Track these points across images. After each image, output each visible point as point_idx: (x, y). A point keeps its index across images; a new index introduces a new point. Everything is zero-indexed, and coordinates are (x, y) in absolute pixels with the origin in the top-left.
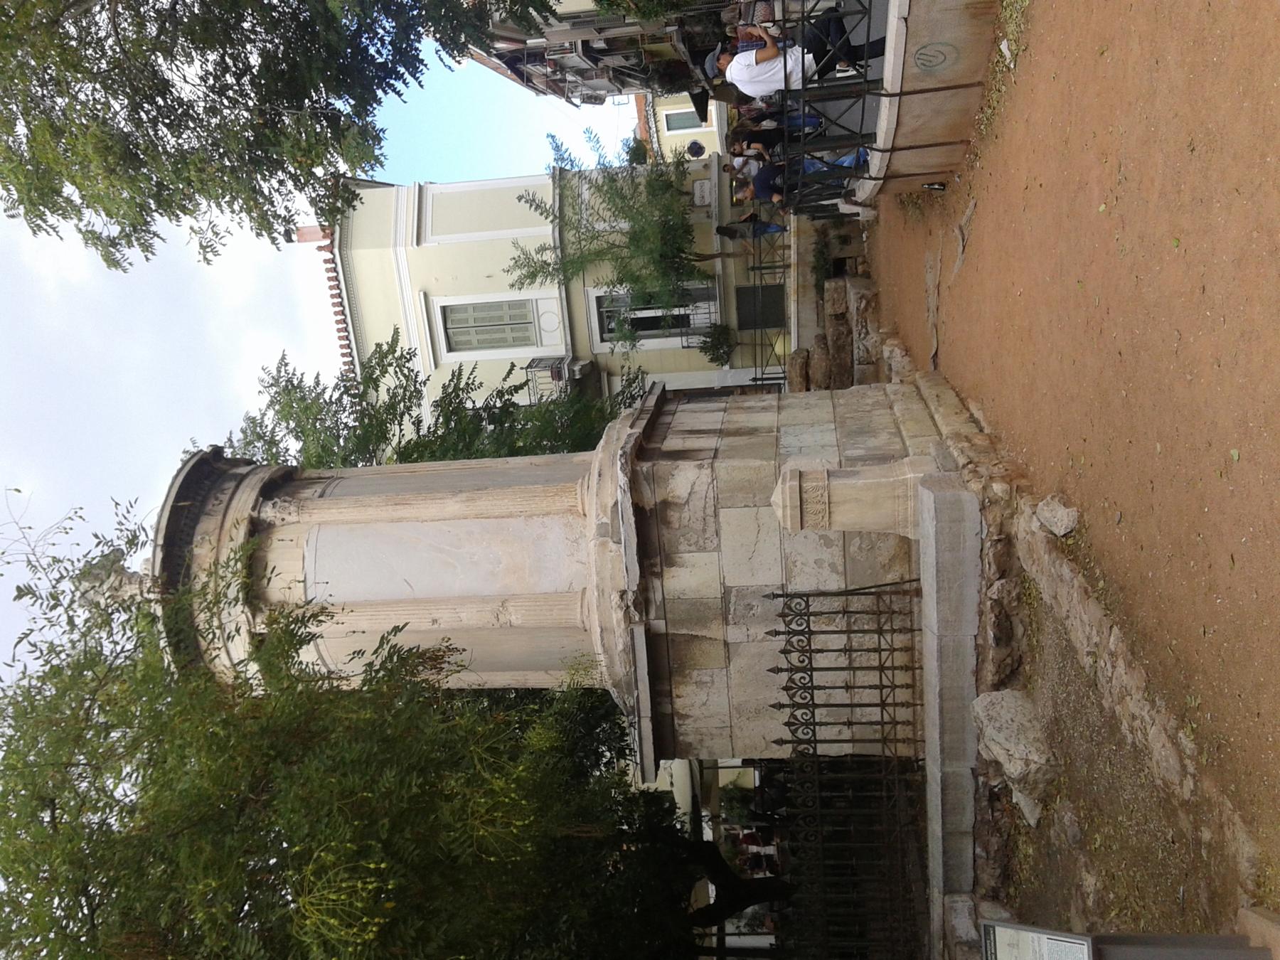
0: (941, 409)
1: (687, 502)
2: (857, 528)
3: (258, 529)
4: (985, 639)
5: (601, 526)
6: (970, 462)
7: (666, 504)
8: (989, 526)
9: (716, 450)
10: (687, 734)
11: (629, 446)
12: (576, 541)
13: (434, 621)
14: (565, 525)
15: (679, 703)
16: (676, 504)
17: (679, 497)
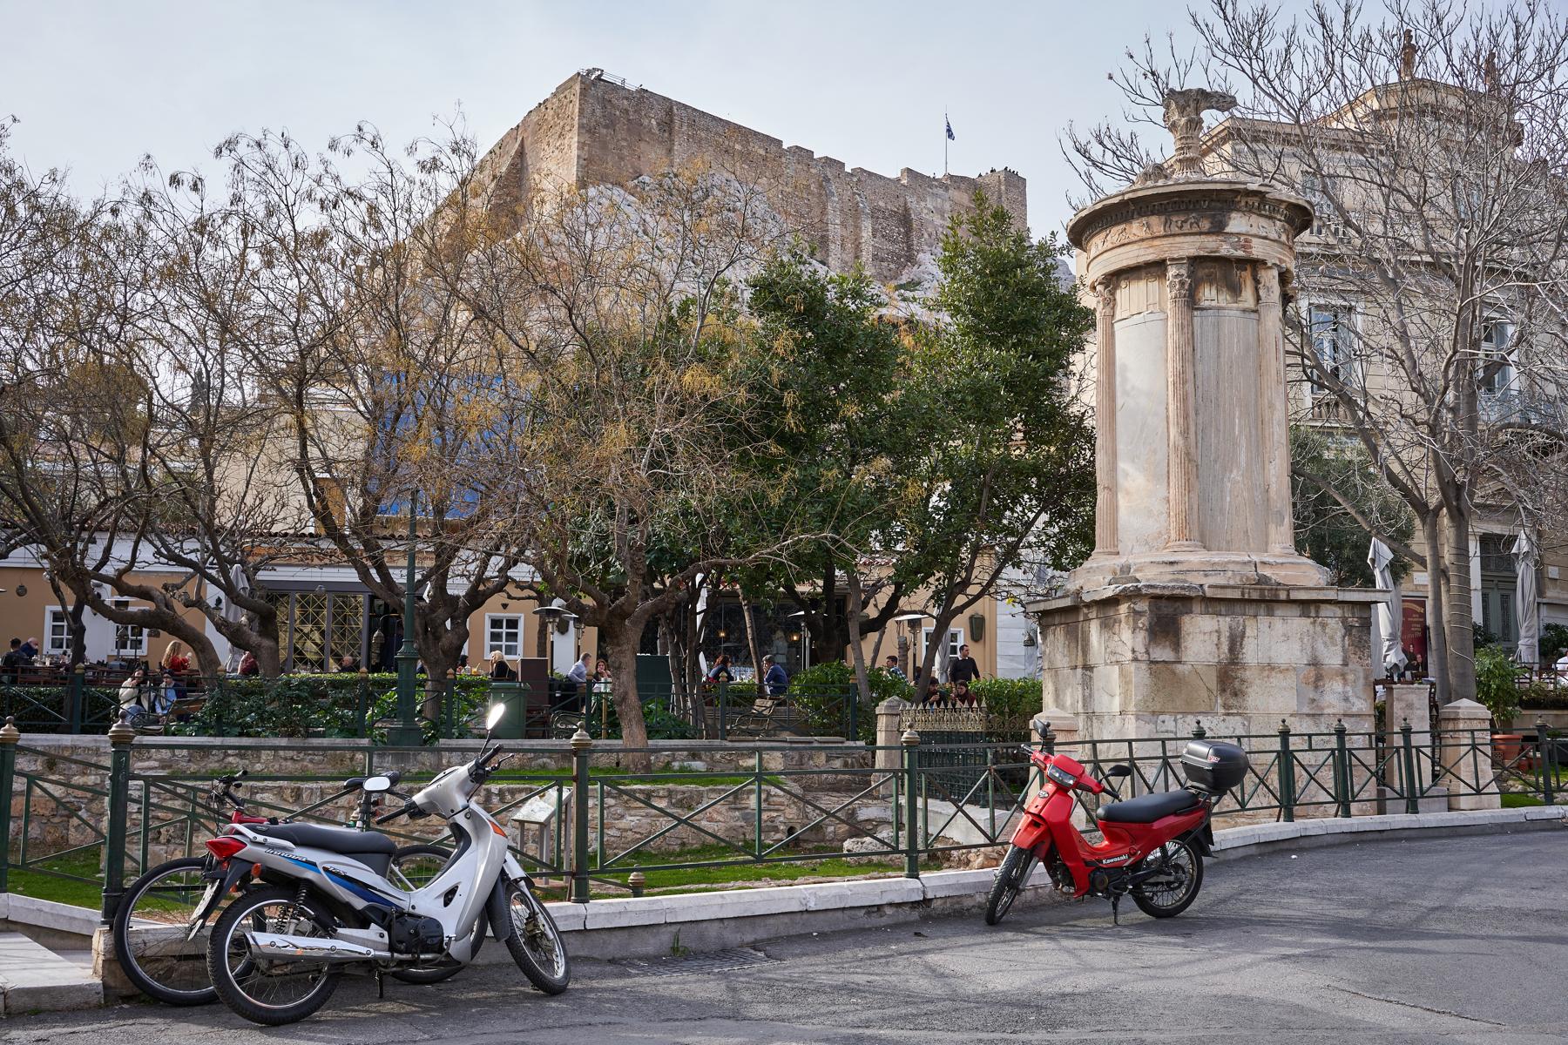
3: (1156, 268)
11: (1151, 591)
12: (1147, 543)
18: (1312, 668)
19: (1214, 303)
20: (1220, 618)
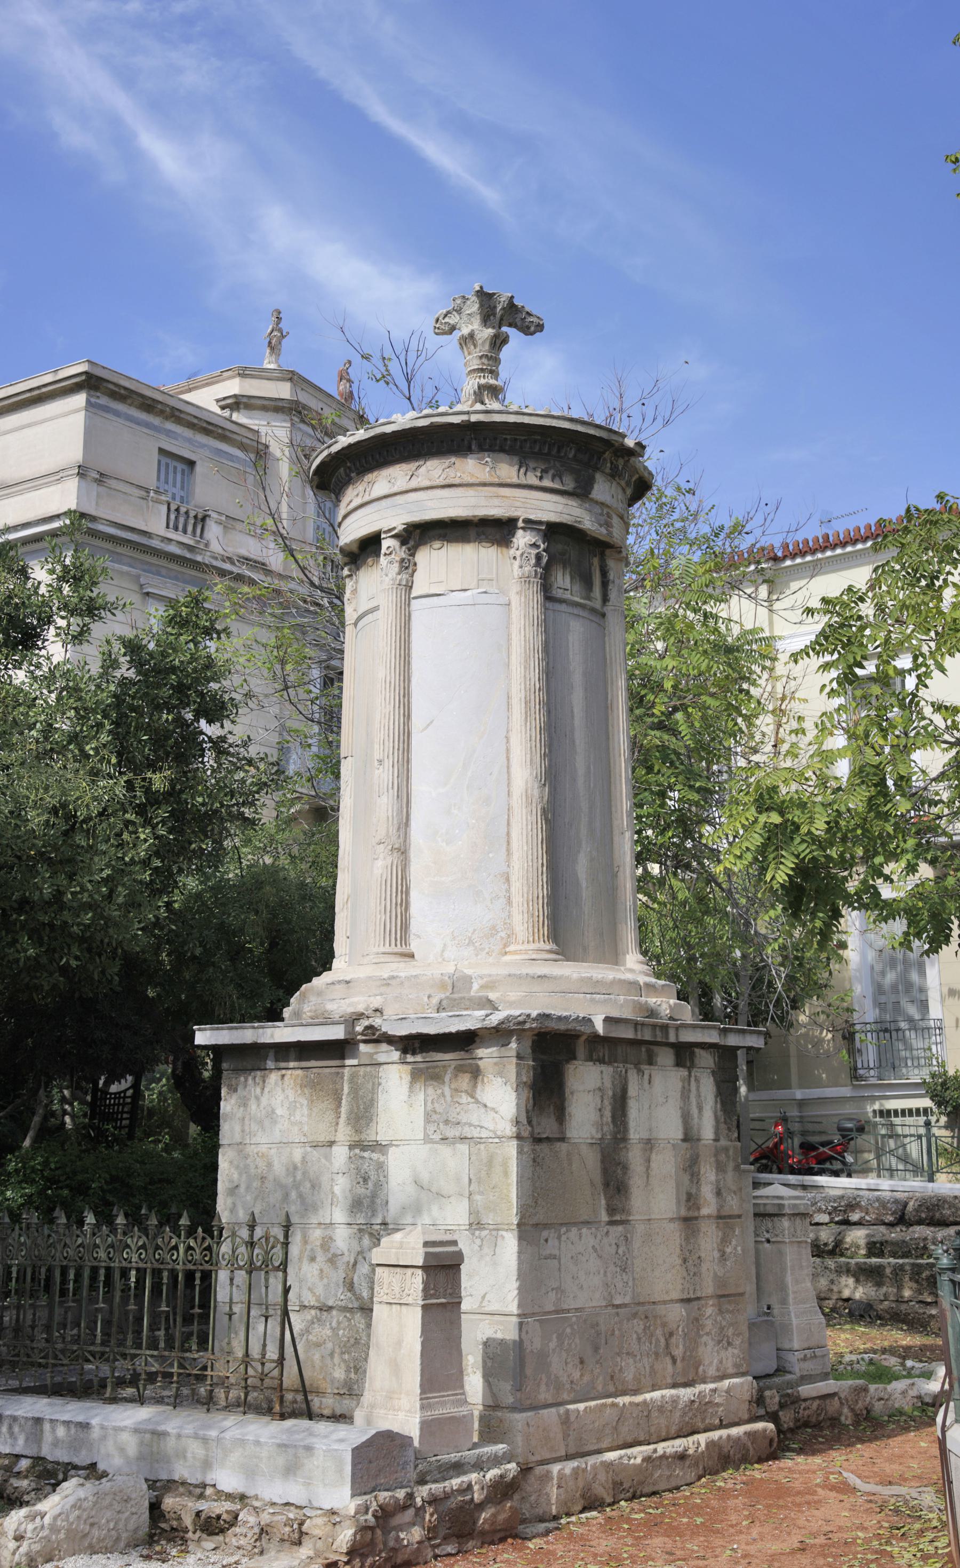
1: (477, 1102)
5: (468, 980)
7: (476, 1073)
9: (562, 1139)
12: (471, 942)
14: (493, 928)
16: (475, 1086)
17: (483, 1090)
18: (685, 1145)
19: (567, 596)
20: (604, 1068)
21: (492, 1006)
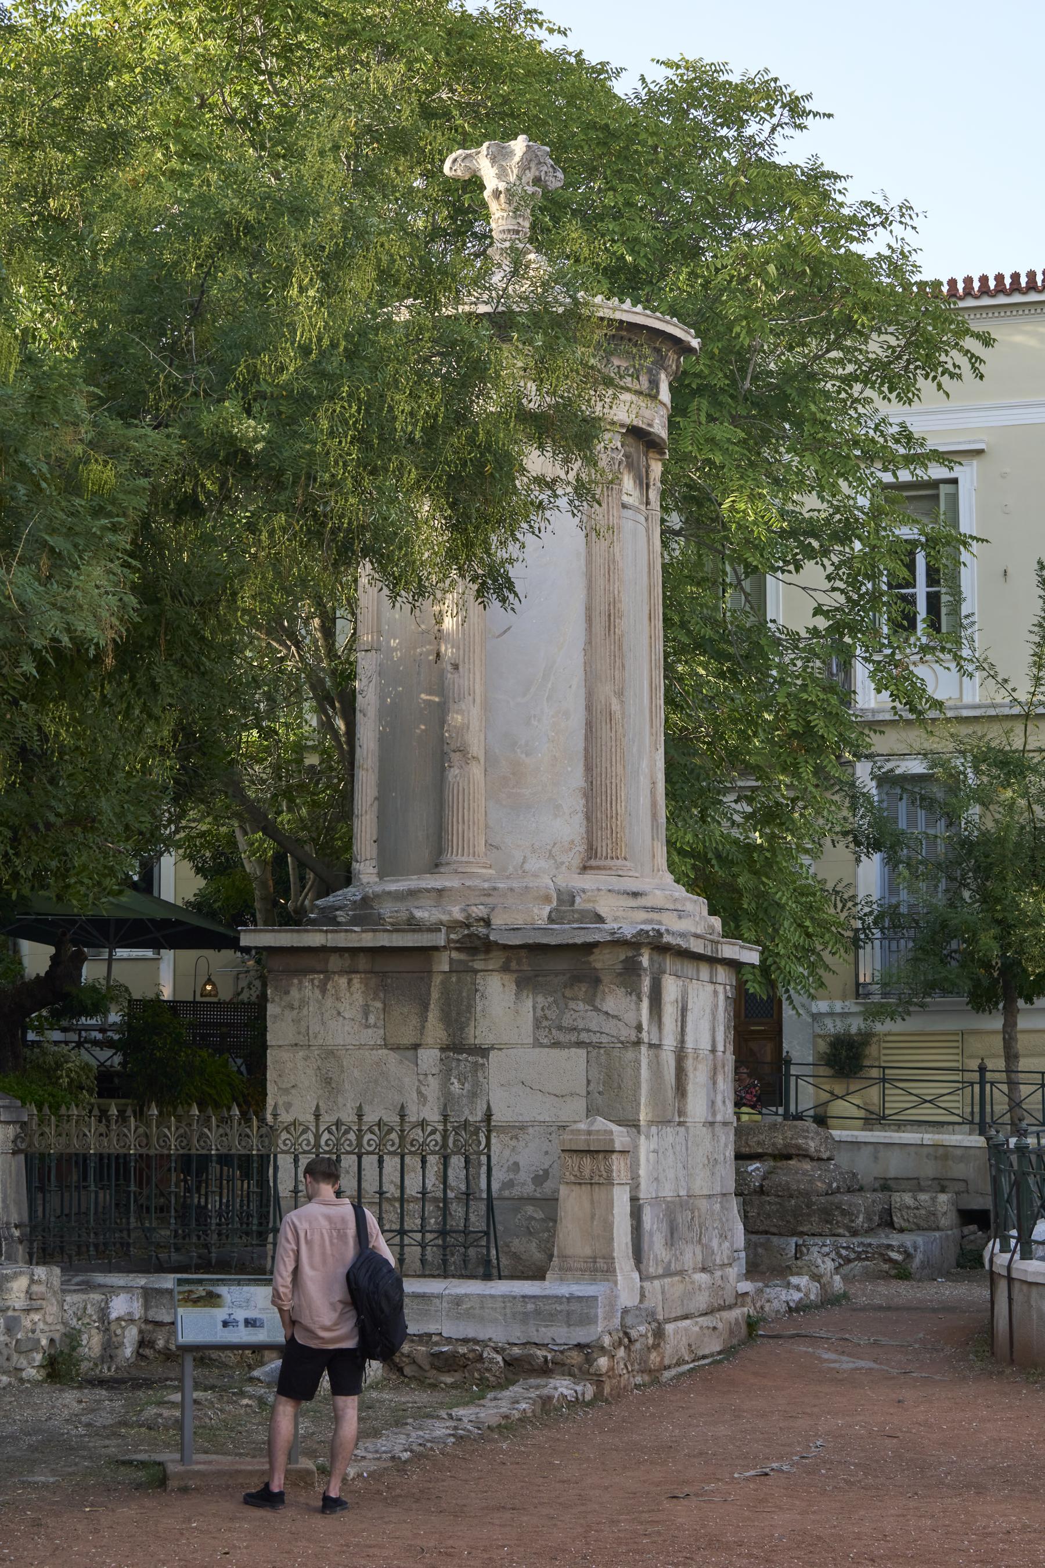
0: (697, 1329)
2: (561, 1213)
4: (436, 1344)
6: (630, 1341)
7: (597, 981)
8: (562, 1352)
10: (300, 990)
12: (551, 856)
13: (456, 667)
15: (343, 981)
16: (594, 995)
17: (603, 1000)
18: (711, 1056)
21: (600, 919)
